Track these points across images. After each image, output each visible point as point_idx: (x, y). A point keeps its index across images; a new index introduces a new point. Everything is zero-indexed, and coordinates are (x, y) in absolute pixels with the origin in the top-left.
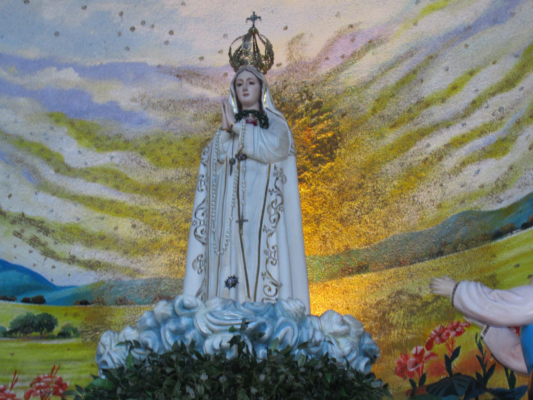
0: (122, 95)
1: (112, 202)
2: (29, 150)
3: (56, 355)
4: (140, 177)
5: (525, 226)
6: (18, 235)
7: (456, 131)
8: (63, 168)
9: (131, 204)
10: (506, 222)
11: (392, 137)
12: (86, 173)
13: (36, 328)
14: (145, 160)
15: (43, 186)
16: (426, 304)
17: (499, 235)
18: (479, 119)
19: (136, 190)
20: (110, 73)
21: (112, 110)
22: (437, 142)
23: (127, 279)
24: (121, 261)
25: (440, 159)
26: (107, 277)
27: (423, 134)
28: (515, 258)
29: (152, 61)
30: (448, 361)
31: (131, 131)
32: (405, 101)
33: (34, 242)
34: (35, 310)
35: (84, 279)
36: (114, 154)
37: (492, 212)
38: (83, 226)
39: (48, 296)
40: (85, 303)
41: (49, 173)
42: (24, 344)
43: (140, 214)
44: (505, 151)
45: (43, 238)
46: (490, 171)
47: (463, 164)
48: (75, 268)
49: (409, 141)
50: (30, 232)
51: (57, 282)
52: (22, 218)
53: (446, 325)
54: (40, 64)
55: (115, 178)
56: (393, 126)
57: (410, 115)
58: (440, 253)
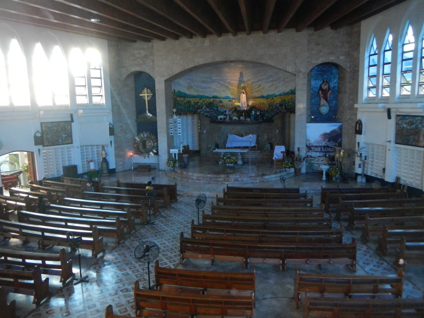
13: (230, 101)
20: (232, 80)
29: (235, 79)
35: (233, 97)
46: (256, 94)
55: (233, 89)
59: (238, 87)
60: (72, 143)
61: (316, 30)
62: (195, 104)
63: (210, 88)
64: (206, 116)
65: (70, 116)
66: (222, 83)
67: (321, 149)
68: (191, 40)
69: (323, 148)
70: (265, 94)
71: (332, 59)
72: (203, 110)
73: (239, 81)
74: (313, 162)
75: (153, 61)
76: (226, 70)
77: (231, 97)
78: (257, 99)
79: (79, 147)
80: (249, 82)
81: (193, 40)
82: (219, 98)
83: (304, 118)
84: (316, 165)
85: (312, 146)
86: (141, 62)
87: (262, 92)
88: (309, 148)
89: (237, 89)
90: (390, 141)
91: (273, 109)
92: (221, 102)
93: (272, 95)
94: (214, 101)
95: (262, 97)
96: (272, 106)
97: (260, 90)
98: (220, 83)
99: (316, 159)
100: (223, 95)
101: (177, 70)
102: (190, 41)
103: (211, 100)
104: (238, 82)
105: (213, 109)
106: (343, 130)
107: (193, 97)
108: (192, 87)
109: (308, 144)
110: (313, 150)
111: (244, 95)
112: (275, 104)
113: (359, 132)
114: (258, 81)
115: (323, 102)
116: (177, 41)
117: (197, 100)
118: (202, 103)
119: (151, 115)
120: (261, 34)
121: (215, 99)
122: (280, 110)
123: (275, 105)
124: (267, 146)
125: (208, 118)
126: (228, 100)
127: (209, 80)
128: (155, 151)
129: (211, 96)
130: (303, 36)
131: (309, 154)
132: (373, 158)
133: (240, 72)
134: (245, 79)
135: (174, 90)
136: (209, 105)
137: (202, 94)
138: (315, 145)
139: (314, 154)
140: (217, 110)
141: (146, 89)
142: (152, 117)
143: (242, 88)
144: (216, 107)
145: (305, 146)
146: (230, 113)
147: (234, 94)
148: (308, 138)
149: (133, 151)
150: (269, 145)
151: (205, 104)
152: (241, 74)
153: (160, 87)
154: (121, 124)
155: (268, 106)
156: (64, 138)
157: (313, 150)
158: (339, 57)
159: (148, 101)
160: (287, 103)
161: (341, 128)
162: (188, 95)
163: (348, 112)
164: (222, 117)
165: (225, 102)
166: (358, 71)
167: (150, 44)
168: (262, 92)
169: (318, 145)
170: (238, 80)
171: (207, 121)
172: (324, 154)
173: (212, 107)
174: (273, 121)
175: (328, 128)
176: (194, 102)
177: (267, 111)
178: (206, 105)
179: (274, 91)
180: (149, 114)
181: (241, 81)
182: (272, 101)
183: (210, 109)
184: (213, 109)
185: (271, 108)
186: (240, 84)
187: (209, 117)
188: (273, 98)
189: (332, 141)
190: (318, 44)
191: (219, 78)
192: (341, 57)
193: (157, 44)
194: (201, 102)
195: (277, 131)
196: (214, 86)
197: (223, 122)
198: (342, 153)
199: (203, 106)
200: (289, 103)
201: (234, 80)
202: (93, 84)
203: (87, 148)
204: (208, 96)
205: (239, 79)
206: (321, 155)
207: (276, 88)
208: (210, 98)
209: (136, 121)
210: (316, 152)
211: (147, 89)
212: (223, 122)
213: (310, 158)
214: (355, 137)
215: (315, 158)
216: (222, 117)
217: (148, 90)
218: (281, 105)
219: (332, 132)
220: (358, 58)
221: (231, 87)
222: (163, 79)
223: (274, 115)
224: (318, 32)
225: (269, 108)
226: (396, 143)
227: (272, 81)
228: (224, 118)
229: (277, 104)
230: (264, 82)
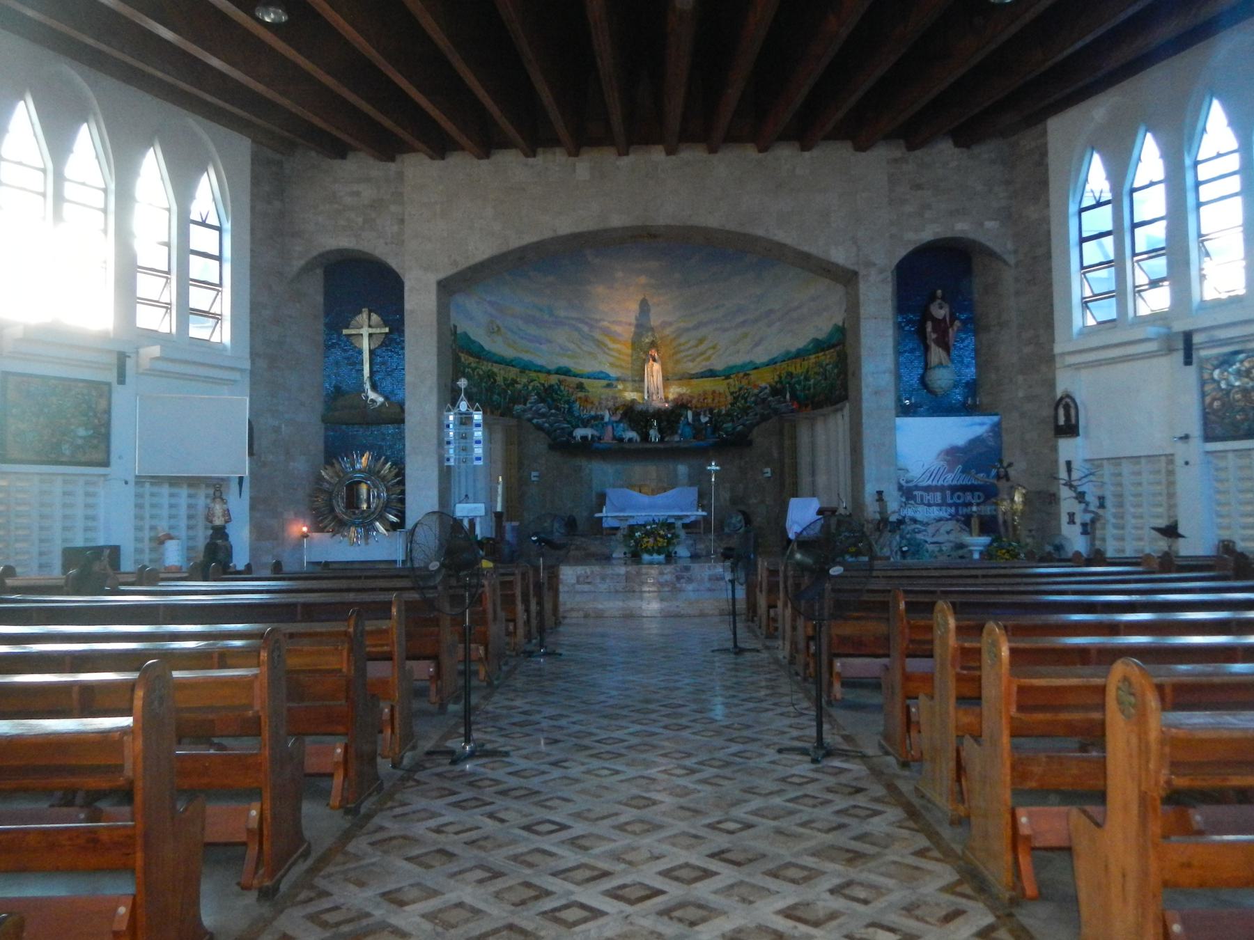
0: (618, 329)
13: (609, 386)
18: (690, 352)
20: (613, 322)
22: (683, 354)
35: (619, 375)
46: (691, 365)
55: (619, 352)
59: (633, 344)
60: (106, 464)
61: (911, 147)
62: (508, 386)
63: (550, 341)
64: (539, 428)
65: (113, 360)
66: (586, 329)
67: (944, 498)
68: (531, 160)
69: (948, 493)
70: (719, 365)
71: (962, 228)
73: (637, 326)
74: (920, 536)
75: (402, 221)
76: (600, 290)
77: (613, 373)
78: (694, 382)
79: (132, 480)
80: (668, 331)
81: (539, 160)
82: (576, 376)
83: (889, 401)
84: (930, 547)
85: (917, 488)
86: (360, 220)
87: (709, 358)
88: (908, 493)
89: (629, 351)
90: (1186, 438)
91: (749, 407)
92: (580, 387)
93: (743, 366)
94: (560, 382)
95: (711, 374)
96: (746, 399)
97: (702, 354)
99: (931, 529)
100: (586, 365)
101: (481, 250)
102: (526, 165)
103: (554, 379)
104: (633, 329)
105: (558, 409)
106: (1006, 438)
107: (502, 361)
108: (499, 329)
109: (903, 483)
110: (919, 500)
111: (657, 367)
112: (756, 391)
113: (1070, 430)
114: (696, 327)
115: (936, 354)
116: (484, 162)
117: (513, 373)
118: (526, 386)
119: (381, 399)
120: (751, 152)
121: (562, 377)
122: (773, 405)
123: (757, 395)
124: (734, 520)
125: (543, 435)
126: (604, 382)
127: (546, 317)
128: (393, 518)
129: (552, 367)
130: (876, 163)
131: (909, 512)
132: (1121, 505)
133: (640, 297)
134: (655, 320)
135: (455, 327)
136: (549, 394)
137: (526, 357)
138: (925, 484)
139: (921, 513)
140: (570, 411)
141: (365, 311)
142: (383, 404)
143: (643, 347)
144: (568, 402)
145: (896, 487)
146: (614, 419)
147: (621, 367)
148: (901, 463)
149: (308, 523)
150: (740, 517)
152: (644, 307)
153: (420, 301)
154: (276, 423)
155: (730, 398)
156: (80, 442)
157: (919, 500)
158: (982, 225)
159: (371, 352)
160: (799, 382)
161: (997, 430)
162: (489, 352)
163: (1020, 378)
164: (588, 432)
165: (595, 388)
166: (1048, 256)
167: (392, 166)
169: (935, 483)
170: (633, 321)
171: (538, 445)
172: (953, 510)
173: (554, 400)
174: (750, 443)
175: (959, 430)
176: (505, 379)
177: (728, 414)
178: (538, 394)
180: (372, 395)
181: (642, 327)
182: (744, 382)
184: (558, 409)
186: (638, 336)
187: (548, 433)
188: (746, 375)
189: (973, 471)
190: (919, 187)
191: (574, 314)
192: (989, 224)
193: (418, 169)
194: (524, 380)
195: (768, 470)
196: (561, 336)
197: (587, 449)
198: (1018, 498)
200: (807, 379)
201: (619, 323)
202: (194, 273)
203: (155, 489)
204: (542, 367)
205: (637, 319)
206: (946, 515)
207: (757, 345)
208: (549, 372)
209: (325, 420)
210: (929, 505)
211: (370, 311)
212: (587, 449)
213: (914, 526)
214: (1055, 449)
215: (927, 524)
216: (588, 432)
217: (375, 317)
218: (776, 391)
219: (976, 442)
220: (1046, 220)
222: (432, 279)
223: (753, 426)
224: (918, 153)
225: (732, 404)
226: (1208, 437)
227: (744, 323)
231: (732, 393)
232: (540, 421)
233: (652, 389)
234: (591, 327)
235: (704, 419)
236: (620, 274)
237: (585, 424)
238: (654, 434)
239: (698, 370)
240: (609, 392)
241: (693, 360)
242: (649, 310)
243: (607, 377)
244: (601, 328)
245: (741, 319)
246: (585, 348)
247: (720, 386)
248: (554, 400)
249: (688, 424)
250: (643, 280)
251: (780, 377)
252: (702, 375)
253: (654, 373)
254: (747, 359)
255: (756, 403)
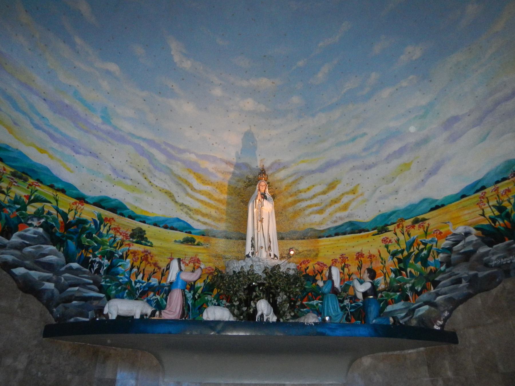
0: (209, 166)
1: (209, 203)
2: (182, 180)
3: (196, 251)
4: (216, 196)
5: (327, 237)
6: (182, 210)
7: (308, 203)
8: (193, 189)
9: (214, 205)
10: (322, 234)
11: (290, 199)
12: (200, 192)
14: (218, 190)
15: (187, 194)
16: (300, 253)
17: (320, 237)
18: (315, 201)
19: (216, 200)
20: (205, 157)
21: (206, 170)
22: (304, 204)
23: (215, 229)
24: (213, 223)
25: (304, 210)
26: (209, 228)
27: (299, 201)
28: (324, 245)
29: (219, 156)
30: (306, 270)
31: (213, 179)
32: (294, 189)
33: (187, 213)
34: (189, 236)
35: (203, 228)
36: (208, 186)
37: (318, 230)
38: (201, 210)
39: (192, 231)
40: (203, 235)
41: (189, 190)
42: (187, 246)
43: (218, 209)
44: (322, 213)
45: (190, 212)
46: (317, 218)
47: (311, 213)
48: (199, 224)
49: (295, 202)
50: (186, 210)
51: (195, 227)
52: (182, 205)
53: (305, 260)
54: (184, 151)
55: (209, 195)
56: (291, 196)
57: (296, 194)
58: (304, 239)
64: (29, 287)
66: (161, 157)
70: (364, 214)
72: (20, 247)
78: (325, 241)
80: (281, 175)
87: (345, 208)
89: (224, 196)
92: (139, 236)
93: (410, 209)
95: (355, 228)
96: (425, 262)
98: (150, 157)
103: (89, 213)
105: (85, 262)
111: (268, 207)
112: (444, 243)
114: (322, 170)
122: (494, 260)
123: (450, 249)
126: (182, 236)
127: (97, 120)
133: (246, 129)
136: (67, 233)
137: (37, 157)
144: (110, 255)
151: (38, 215)
155: (391, 264)
165: (161, 240)
168: (345, 208)
173: (80, 246)
177: (390, 288)
179: (416, 188)
182: (416, 233)
183: (69, 259)
184: (85, 262)
185: (415, 268)
187: (49, 303)
188: (416, 221)
194: (20, 191)
196: (119, 156)
199: (23, 220)
204: (71, 186)
208: (82, 199)
216: (136, 308)
221: (196, 184)
225: (397, 272)
227: (401, 152)
228: (142, 316)
229: (458, 239)
230: (354, 168)
231: (394, 255)
232: (35, 274)
233: (260, 242)
234: (170, 156)
235: (361, 288)
236: (218, 92)
237: (133, 294)
238: (263, 307)
239: (329, 225)
240: (190, 251)
241: (321, 211)
242: (255, 148)
243: (187, 228)
244: (184, 162)
245: (396, 146)
246: (156, 183)
247: (371, 245)
248: (80, 246)
249: (334, 291)
250: (249, 104)
251: (501, 208)
252: (337, 232)
253: (263, 217)
254: (415, 198)
255: (449, 263)
